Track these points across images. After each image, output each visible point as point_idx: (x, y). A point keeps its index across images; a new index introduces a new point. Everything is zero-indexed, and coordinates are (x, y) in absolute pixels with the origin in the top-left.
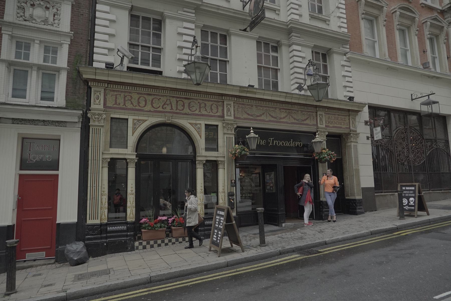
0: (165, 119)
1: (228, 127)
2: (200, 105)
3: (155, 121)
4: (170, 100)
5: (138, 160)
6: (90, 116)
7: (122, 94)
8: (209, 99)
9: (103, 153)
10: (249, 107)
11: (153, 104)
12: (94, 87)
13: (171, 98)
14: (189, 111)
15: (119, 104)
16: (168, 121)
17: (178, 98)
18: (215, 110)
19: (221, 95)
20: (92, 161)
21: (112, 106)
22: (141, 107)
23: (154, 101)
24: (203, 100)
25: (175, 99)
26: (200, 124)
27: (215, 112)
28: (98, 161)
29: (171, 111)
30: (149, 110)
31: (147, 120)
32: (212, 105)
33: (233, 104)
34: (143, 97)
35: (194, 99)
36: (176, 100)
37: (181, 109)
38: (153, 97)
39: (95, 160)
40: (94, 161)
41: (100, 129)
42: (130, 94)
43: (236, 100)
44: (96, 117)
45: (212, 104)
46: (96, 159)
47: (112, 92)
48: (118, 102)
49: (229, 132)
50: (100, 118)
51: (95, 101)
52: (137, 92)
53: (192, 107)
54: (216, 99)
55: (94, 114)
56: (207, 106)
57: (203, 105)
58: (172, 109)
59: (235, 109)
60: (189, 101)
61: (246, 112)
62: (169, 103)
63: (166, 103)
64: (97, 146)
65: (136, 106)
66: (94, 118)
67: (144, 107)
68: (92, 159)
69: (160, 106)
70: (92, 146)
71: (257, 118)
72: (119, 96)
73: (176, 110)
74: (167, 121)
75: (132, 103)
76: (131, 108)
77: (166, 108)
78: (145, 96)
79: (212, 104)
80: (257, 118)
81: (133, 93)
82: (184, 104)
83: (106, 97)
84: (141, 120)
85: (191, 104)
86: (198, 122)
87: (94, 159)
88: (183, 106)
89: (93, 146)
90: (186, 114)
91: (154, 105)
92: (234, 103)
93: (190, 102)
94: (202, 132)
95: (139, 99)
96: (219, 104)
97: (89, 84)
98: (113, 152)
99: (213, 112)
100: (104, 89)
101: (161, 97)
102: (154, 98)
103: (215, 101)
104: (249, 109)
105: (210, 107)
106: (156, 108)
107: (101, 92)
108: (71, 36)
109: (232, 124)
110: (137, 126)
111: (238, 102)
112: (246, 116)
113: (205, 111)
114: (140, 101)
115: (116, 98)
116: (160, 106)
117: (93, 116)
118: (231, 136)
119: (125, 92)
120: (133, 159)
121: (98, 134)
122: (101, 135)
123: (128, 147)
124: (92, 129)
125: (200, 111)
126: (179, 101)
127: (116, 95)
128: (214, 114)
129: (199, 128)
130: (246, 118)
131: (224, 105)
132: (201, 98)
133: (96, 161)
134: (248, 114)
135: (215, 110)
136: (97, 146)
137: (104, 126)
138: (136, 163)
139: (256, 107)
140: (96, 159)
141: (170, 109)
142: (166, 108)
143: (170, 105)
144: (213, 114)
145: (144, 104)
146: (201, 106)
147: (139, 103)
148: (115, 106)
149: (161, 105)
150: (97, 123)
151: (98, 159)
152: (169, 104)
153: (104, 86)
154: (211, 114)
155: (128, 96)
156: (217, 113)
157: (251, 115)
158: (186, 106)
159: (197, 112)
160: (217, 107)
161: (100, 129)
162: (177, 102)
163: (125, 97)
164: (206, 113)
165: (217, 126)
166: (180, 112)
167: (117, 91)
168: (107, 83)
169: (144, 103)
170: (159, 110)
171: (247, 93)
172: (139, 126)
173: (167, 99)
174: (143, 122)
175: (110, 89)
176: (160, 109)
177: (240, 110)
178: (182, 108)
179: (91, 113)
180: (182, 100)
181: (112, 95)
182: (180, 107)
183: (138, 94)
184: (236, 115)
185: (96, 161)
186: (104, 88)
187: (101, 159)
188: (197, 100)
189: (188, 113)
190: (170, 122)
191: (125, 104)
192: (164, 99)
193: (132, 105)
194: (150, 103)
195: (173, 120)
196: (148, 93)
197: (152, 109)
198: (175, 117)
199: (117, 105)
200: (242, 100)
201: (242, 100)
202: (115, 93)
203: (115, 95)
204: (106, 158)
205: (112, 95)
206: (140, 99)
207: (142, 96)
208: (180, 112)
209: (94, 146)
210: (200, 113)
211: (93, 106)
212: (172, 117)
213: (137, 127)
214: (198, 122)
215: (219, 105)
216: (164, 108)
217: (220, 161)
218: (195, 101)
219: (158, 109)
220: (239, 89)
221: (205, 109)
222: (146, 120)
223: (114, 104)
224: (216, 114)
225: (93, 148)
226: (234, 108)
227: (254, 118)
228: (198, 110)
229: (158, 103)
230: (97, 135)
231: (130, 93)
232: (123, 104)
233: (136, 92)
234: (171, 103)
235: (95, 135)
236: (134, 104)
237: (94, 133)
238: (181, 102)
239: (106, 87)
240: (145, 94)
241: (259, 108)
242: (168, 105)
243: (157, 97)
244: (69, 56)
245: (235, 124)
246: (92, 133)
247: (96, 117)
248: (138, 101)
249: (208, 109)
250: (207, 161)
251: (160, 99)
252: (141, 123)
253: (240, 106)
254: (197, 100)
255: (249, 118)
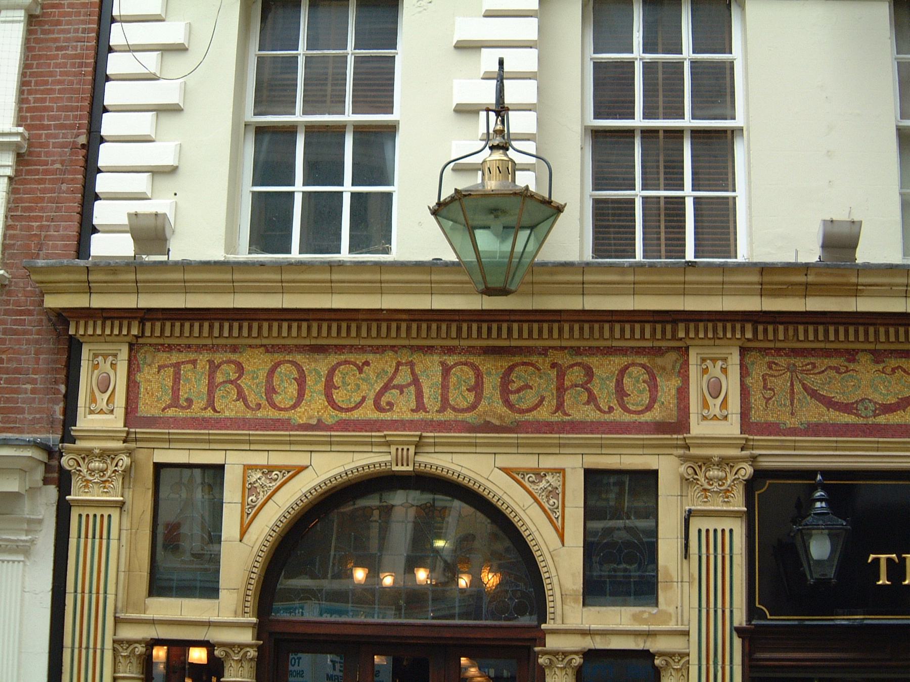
0: (388, 458)
1: (709, 480)
2: (561, 376)
3: (341, 470)
4: (411, 364)
5: (260, 649)
6: (72, 463)
7: (203, 359)
8: (608, 343)
9: (117, 621)
10: (834, 362)
11: (334, 391)
12: (91, 339)
13: (416, 358)
14: (502, 409)
15: (190, 401)
16: (400, 468)
17: (450, 350)
18: (638, 395)
19: (670, 319)
20: (76, 651)
21: (156, 412)
22: (281, 409)
23: (337, 380)
24: (577, 351)
25: (436, 358)
26: (561, 471)
27: (640, 408)
28: (99, 652)
29: (416, 416)
30: (314, 422)
31: (305, 468)
32: (623, 371)
33: (735, 359)
34: (289, 362)
35: (529, 351)
36: (443, 364)
37: (464, 405)
38: (333, 359)
39: (87, 648)
40: (84, 652)
41: (110, 516)
42: (234, 357)
43: (749, 335)
44: (92, 465)
45: (627, 367)
46: (91, 646)
47: (160, 354)
48: (183, 394)
49: (717, 505)
50: (111, 468)
51: (93, 400)
52: (265, 342)
53: (518, 391)
54: (643, 337)
55: (88, 454)
56: (596, 381)
57: (575, 376)
58: (420, 406)
59: (749, 381)
60: (505, 363)
61: (814, 394)
62: (409, 379)
63: (395, 382)
64: (94, 590)
65: (259, 406)
66: (88, 469)
67: (294, 407)
68: (77, 645)
69: (364, 399)
70: (76, 591)
71: (882, 419)
72: (190, 366)
73: (442, 410)
74: (395, 468)
75: (241, 396)
76: (240, 415)
77: (389, 404)
78: (299, 358)
79: (627, 367)
80: (882, 419)
81: (249, 351)
82: (479, 376)
83: (139, 377)
84: (280, 468)
85: (513, 376)
86: (548, 462)
87: (84, 645)
88: (477, 388)
89: (79, 590)
90: (487, 427)
91: (338, 396)
92: (743, 351)
93: (511, 369)
94: (567, 510)
95: (272, 371)
96: (659, 361)
97: (72, 332)
98: (157, 617)
99: (631, 407)
100: (131, 346)
101: (370, 357)
102: (339, 364)
103: (639, 351)
104: (833, 373)
105: (613, 384)
106: (348, 410)
107: (119, 358)
108: (17, 144)
109: (725, 462)
110: (262, 498)
111: (771, 345)
112: (814, 413)
113: (588, 403)
114: (276, 382)
115: (177, 378)
116: (364, 399)
117: (81, 462)
118: (726, 524)
119: (213, 349)
120: (241, 646)
121: (101, 538)
122: (114, 544)
123: (222, 593)
124: (80, 516)
125: (560, 407)
126: (456, 364)
127: (177, 366)
128: (635, 417)
129: (552, 492)
130: (817, 425)
131: (686, 362)
132: (564, 344)
133: (91, 651)
134: (829, 403)
135: (638, 395)
136: (94, 590)
137: (123, 503)
138: (260, 661)
139: (878, 362)
140: (91, 646)
141: (413, 410)
142: (390, 404)
143: (412, 388)
144: (627, 418)
145: (295, 394)
146: (567, 383)
147: (271, 390)
148: (171, 413)
149: (372, 395)
150: (96, 495)
151: (99, 646)
152: (409, 385)
153: (125, 332)
154: (619, 415)
155: (224, 367)
156: (649, 408)
157: (847, 408)
158: (487, 392)
159: (544, 414)
160: (653, 378)
161: (110, 516)
162: (446, 371)
163: (214, 368)
164: (590, 414)
165: (653, 475)
166: (460, 417)
167: (179, 348)
168: (135, 318)
169: (293, 389)
170: (362, 417)
171: (805, 297)
172: (270, 498)
173: (399, 364)
174: (287, 475)
175: (154, 341)
176: (368, 413)
177: (781, 383)
178: (471, 397)
179: (79, 451)
180: (472, 359)
181: (160, 368)
182: (461, 397)
183: (267, 351)
184: (754, 417)
185: (91, 651)
186: (128, 339)
187: (109, 645)
188: (546, 355)
189: (497, 423)
190: (410, 468)
191: (211, 404)
192: (384, 364)
193: (240, 404)
194: (320, 387)
195: (420, 458)
196: (313, 342)
197: (331, 416)
198: (435, 444)
199: (183, 408)
200: (791, 332)
201: (791, 332)
202: (175, 358)
203: (172, 365)
204: (130, 642)
205: (160, 368)
206: (276, 375)
207: (287, 358)
208: (460, 417)
209: (90, 592)
210: (558, 417)
211: (85, 421)
212: (417, 445)
213: (260, 502)
214: (548, 462)
215: (664, 369)
216: (383, 402)
217: (662, 654)
218: (534, 359)
219: (356, 415)
220: (755, 278)
221: (585, 397)
222: (302, 469)
223: (169, 406)
224: (647, 417)
225: (79, 597)
226: (744, 372)
227: (861, 421)
228: (550, 402)
229: (358, 386)
230: (97, 541)
231: (234, 349)
232: (202, 404)
233: (258, 342)
234: (416, 382)
235: (90, 541)
236: (249, 399)
237: (87, 537)
238: (465, 368)
239: (137, 337)
240: (300, 349)
241: (893, 362)
242: (401, 388)
243: (351, 357)
244: (10, 222)
245: (743, 459)
246: (79, 537)
247: (92, 465)
248: (267, 381)
249: (604, 391)
250: (590, 655)
251: (367, 363)
252: (278, 483)
253: (782, 361)
254: (544, 351)
255: (833, 425)
